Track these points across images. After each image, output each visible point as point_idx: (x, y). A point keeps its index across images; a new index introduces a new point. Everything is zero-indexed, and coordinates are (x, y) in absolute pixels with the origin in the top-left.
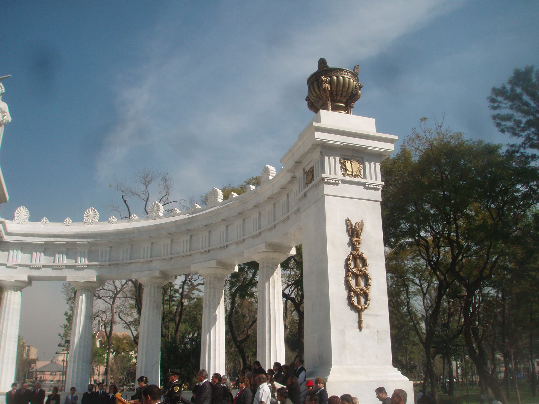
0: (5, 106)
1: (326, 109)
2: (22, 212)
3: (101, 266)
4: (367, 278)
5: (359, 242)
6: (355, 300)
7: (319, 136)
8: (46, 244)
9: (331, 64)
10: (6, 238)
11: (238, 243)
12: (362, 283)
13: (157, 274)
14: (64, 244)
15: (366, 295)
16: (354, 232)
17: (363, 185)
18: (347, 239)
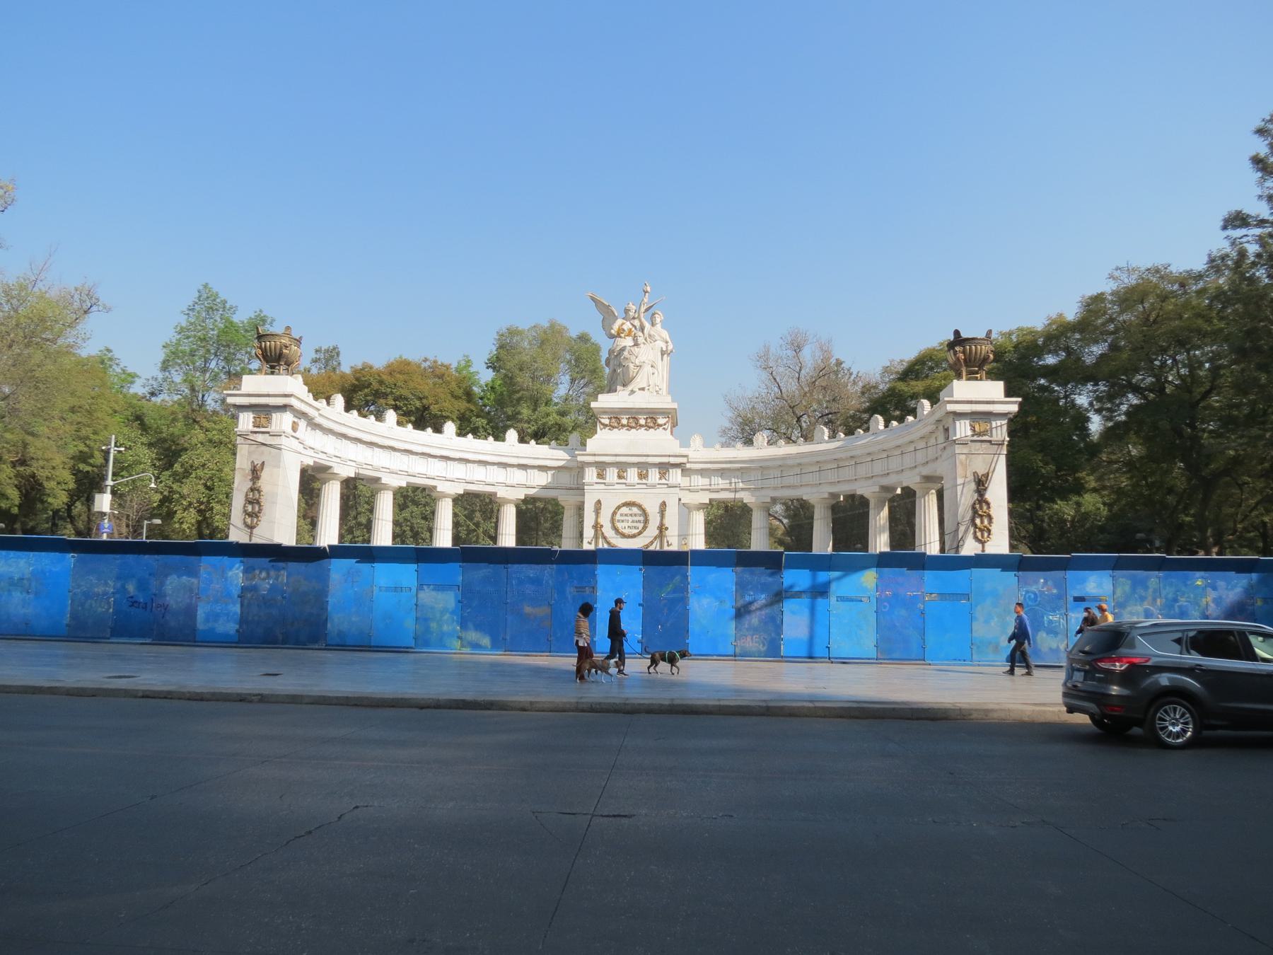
0: (665, 334)
1: (959, 376)
2: (697, 441)
3: (775, 488)
4: (990, 518)
5: (986, 489)
6: (979, 534)
7: (950, 407)
8: (723, 469)
9: (964, 335)
10: (688, 466)
11: (897, 472)
12: (986, 522)
13: (826, 496)
14: (738, 470)
15: (989, 531)
16: (981, 483)
17: (990, 442)
18: (973, 486)
